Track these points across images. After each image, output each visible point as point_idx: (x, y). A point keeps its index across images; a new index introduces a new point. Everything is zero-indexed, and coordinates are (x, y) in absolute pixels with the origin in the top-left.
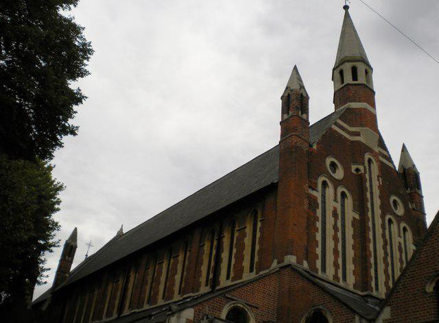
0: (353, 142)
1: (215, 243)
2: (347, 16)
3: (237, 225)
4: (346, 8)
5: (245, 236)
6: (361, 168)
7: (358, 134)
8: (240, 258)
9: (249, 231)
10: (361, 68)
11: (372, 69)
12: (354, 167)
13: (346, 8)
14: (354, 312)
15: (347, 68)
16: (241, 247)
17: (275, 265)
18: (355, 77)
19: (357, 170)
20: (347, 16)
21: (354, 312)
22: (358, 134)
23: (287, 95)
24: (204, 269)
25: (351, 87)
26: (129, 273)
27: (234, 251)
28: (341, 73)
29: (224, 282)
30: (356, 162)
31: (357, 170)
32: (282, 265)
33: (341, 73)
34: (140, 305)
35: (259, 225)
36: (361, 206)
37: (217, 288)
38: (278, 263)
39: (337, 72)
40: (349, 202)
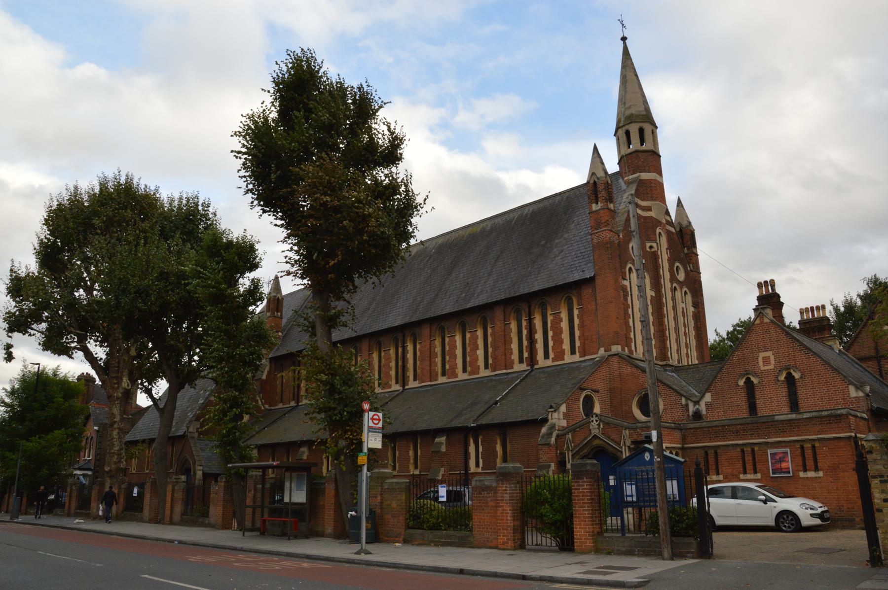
0: (646, 218)
1: (524, 323)
2: (626, 53)
3: (549, 308)
4: (624, 39)
5: (561, 320)
6: (654, 245)
7: (649, 209)
8: (558, 341)
9: (564, 315)
10: (648, 128)
11: (656, 127)
12: (648, 245)
13: (624, 39)
14: (682, 395)
15: (634, 129)
16: (558, 332)
17: (602, 351)
18: (642, 141)
19: (651, 247)
20: (626, 53)
21: (682, 395)
22: (649, 209)
23: (592, 182)
24: (515, 346)
25: (640, 154)
26: (404, 342)
27: (550, 334)
28: (628, 133)
29: (541, 362)
30: (650, 240)
31: (651, 247)
32: (609, 353)
33: (628, 133)
34: (433, 376)
35: (576, 312)
36: (657, 285)
37: (536, 367)
38: (605, 351)
39: (621, 132)
40: (648, 281)
